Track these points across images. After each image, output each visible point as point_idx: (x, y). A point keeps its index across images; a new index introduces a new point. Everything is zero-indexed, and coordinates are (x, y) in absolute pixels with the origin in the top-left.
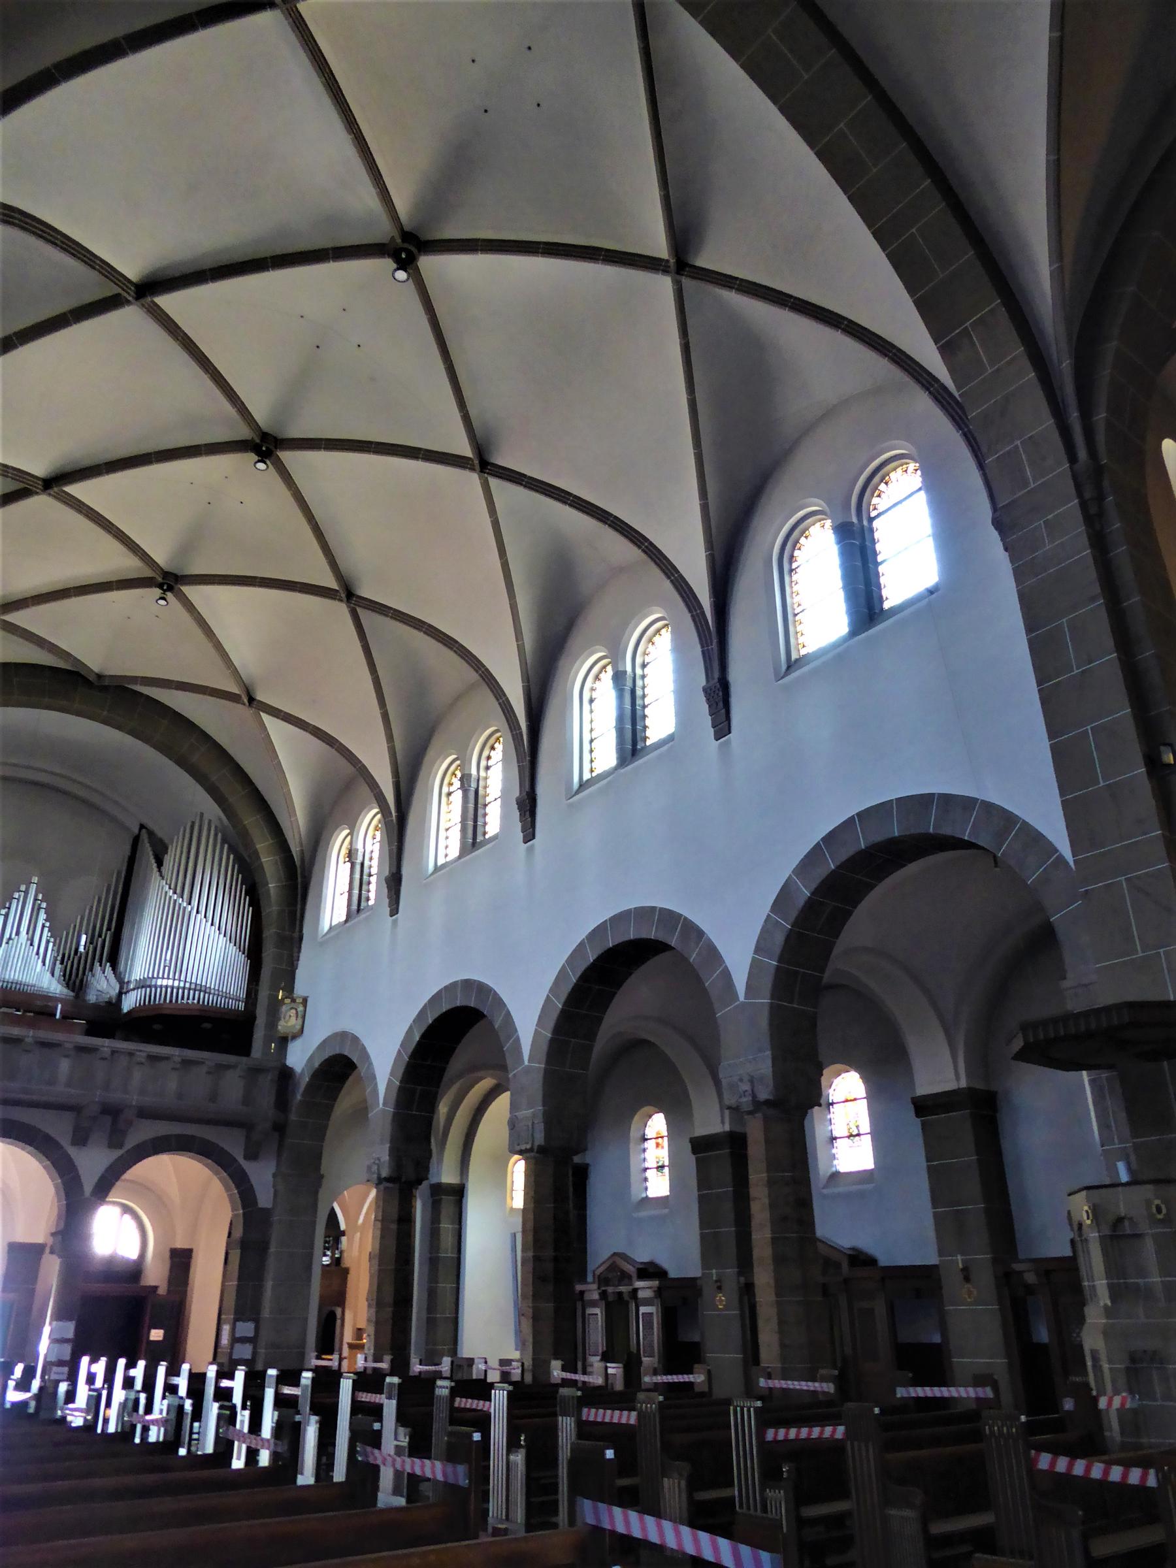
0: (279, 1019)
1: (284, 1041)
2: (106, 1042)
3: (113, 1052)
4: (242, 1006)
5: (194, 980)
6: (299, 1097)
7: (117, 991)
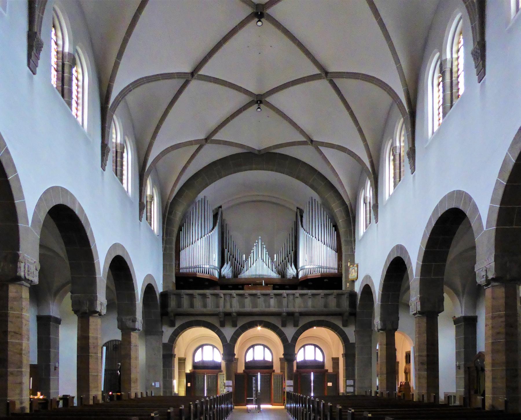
0: (349, 274)
1: (353, 282)
2: (284, 291)
3: (287, 295)
4: (336, 271)
5: (317, 264)
6: (358, 303)
7: (296, 273)
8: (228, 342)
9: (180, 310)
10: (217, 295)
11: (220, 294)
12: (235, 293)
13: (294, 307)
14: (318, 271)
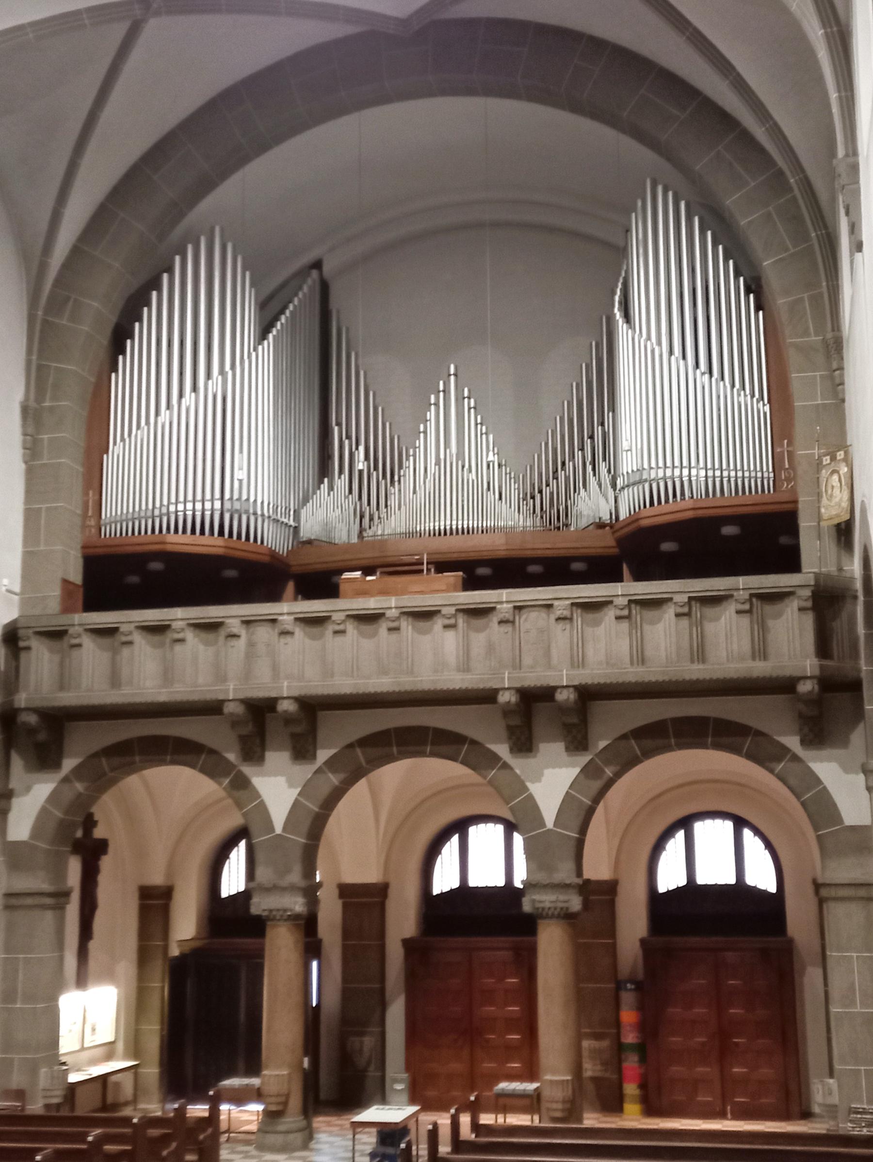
2: (504, 594)
8: (279, 829)
9: (69, 699)
11: (228, 621)
12: (288, 614)
13: (549, 666)
14: (675, 495)
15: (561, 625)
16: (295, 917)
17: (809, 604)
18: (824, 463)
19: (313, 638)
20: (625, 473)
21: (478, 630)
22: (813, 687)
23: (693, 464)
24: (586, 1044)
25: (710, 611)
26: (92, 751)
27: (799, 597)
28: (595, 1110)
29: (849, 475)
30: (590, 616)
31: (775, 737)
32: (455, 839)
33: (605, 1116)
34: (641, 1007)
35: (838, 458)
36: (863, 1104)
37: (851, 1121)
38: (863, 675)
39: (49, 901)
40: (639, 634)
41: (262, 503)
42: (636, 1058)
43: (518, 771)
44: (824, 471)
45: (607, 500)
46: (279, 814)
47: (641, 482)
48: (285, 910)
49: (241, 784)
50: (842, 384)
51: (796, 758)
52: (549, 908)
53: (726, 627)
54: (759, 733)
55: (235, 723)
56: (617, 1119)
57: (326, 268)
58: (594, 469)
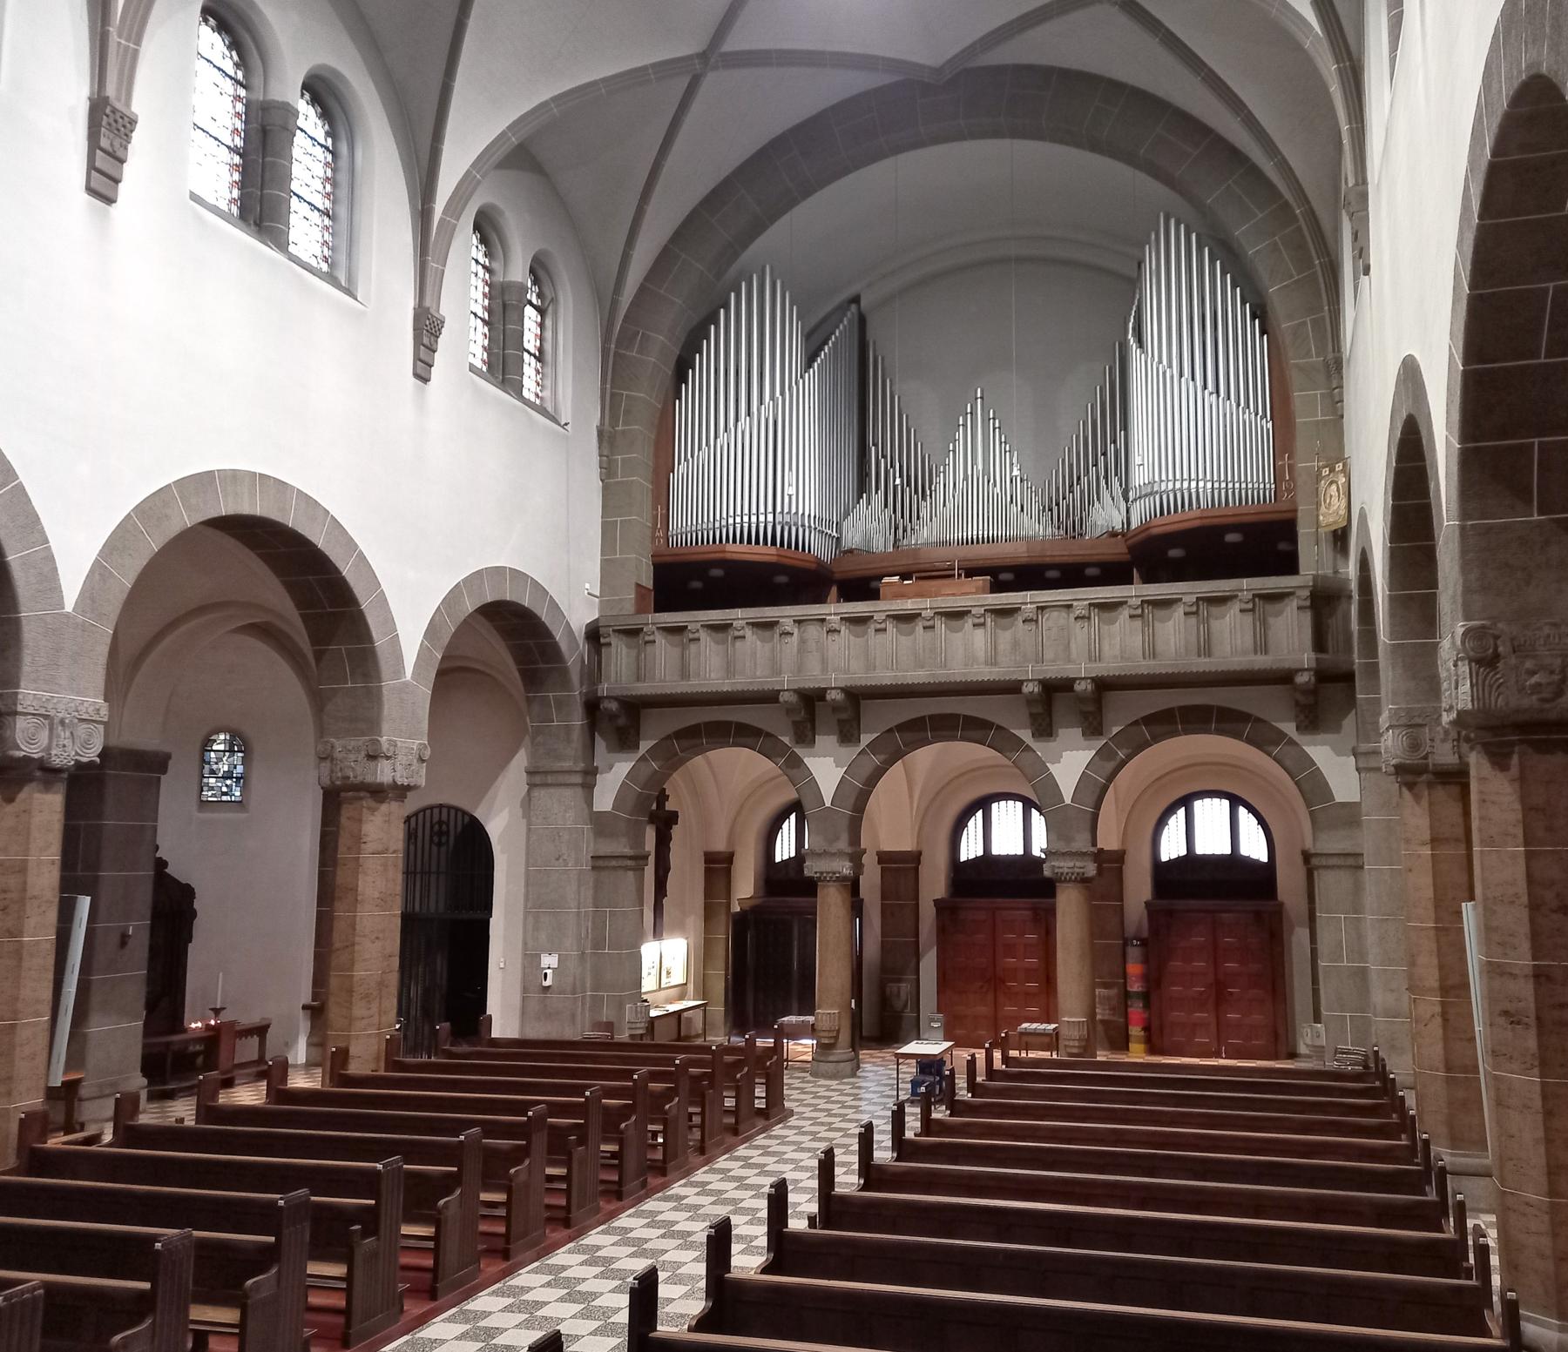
8: (828, 804)
9: (644, 688)
10: (722, 628)
12: (835, 614)
13: (1069, 661)
15: (1080, 623)
16: (842, 879)
17: (1308, 603)
18: (1324, 474)
19: (857, 636)
20: (1137, 486)
21: (1005, 629)
22: (1310, 679)
23: (1200, 477)
24: (1097, 991)
25: (1215, 610)
26: (667, 734)
27: (1298, 597)
28: (1104, 1049)
29: (1347, 484)
30: (1106, 615)
31: (1274, 724)
32: (979, 814)
33: (1113, 1054)
34: (1146, 960)
35: (1337, 469)
36: (1348, 1045)
37: (1336, 1060)
38: (1356, 667)
39: (629, 863)
40: (1151, 631)
41: (809, 515)
42: (1141, 1005)
43: (1040, 754)
44: (1323, 482)
45: (1119, 511)
46: (828, 789)
47: (1152, 493)
48: (834, 873)
49: (795, 763)
50: (1342, 401)
51: (1292, 742)
52: (1067, 874)
53: (1230, 624)
54: (1258, 720)
55: (790, 710)
56: (1124, 1056)
57: (863, 303)
58: (1107, 483)
